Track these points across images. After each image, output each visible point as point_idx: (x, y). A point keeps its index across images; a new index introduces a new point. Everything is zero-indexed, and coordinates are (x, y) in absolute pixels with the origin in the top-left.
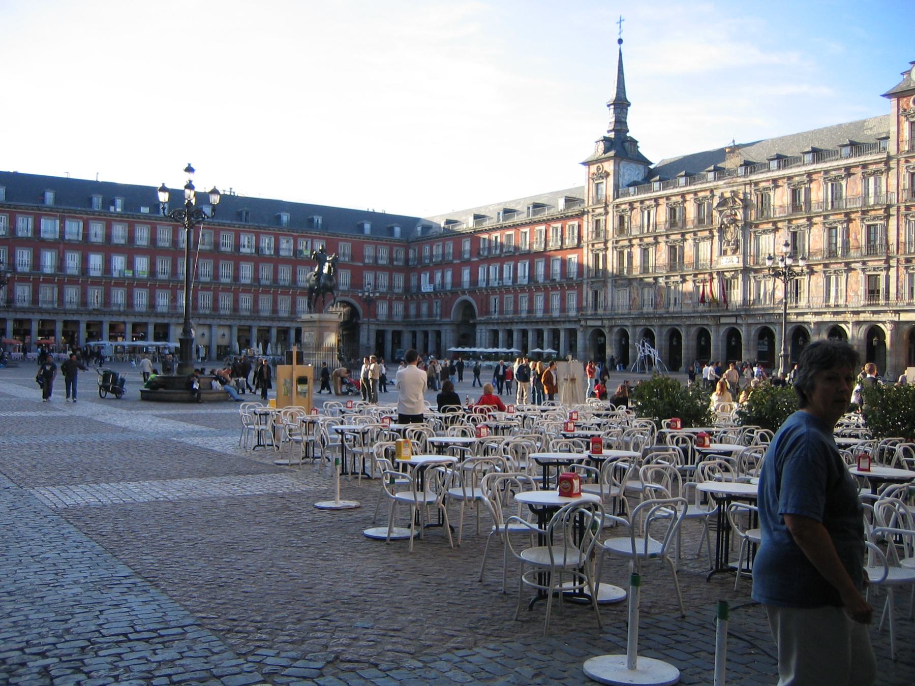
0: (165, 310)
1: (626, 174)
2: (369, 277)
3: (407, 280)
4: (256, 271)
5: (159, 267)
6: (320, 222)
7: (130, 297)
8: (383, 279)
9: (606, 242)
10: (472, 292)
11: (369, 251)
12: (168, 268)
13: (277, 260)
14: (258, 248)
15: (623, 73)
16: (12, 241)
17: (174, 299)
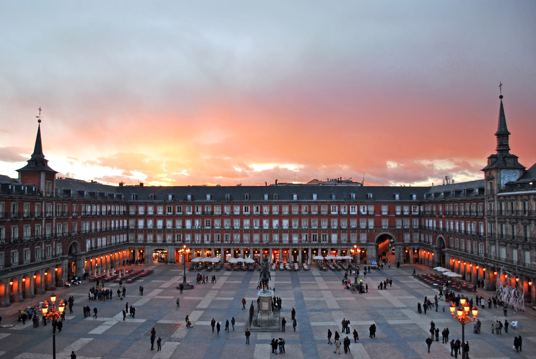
0: (297, 242)
1: (506, 177)
2: (398, 223)
3: (420, 222)
4: (339, 222)
5: (293, 223)
6: (371, 196)
7: (281, 237)
8: (407, 223)
9: (494, 218)
10: (443, 234)
11: (398, 209)
12: (297, 224)
13: (349, 217)
14: (339, 211)
15: (504, 116)
17: (300, 237)
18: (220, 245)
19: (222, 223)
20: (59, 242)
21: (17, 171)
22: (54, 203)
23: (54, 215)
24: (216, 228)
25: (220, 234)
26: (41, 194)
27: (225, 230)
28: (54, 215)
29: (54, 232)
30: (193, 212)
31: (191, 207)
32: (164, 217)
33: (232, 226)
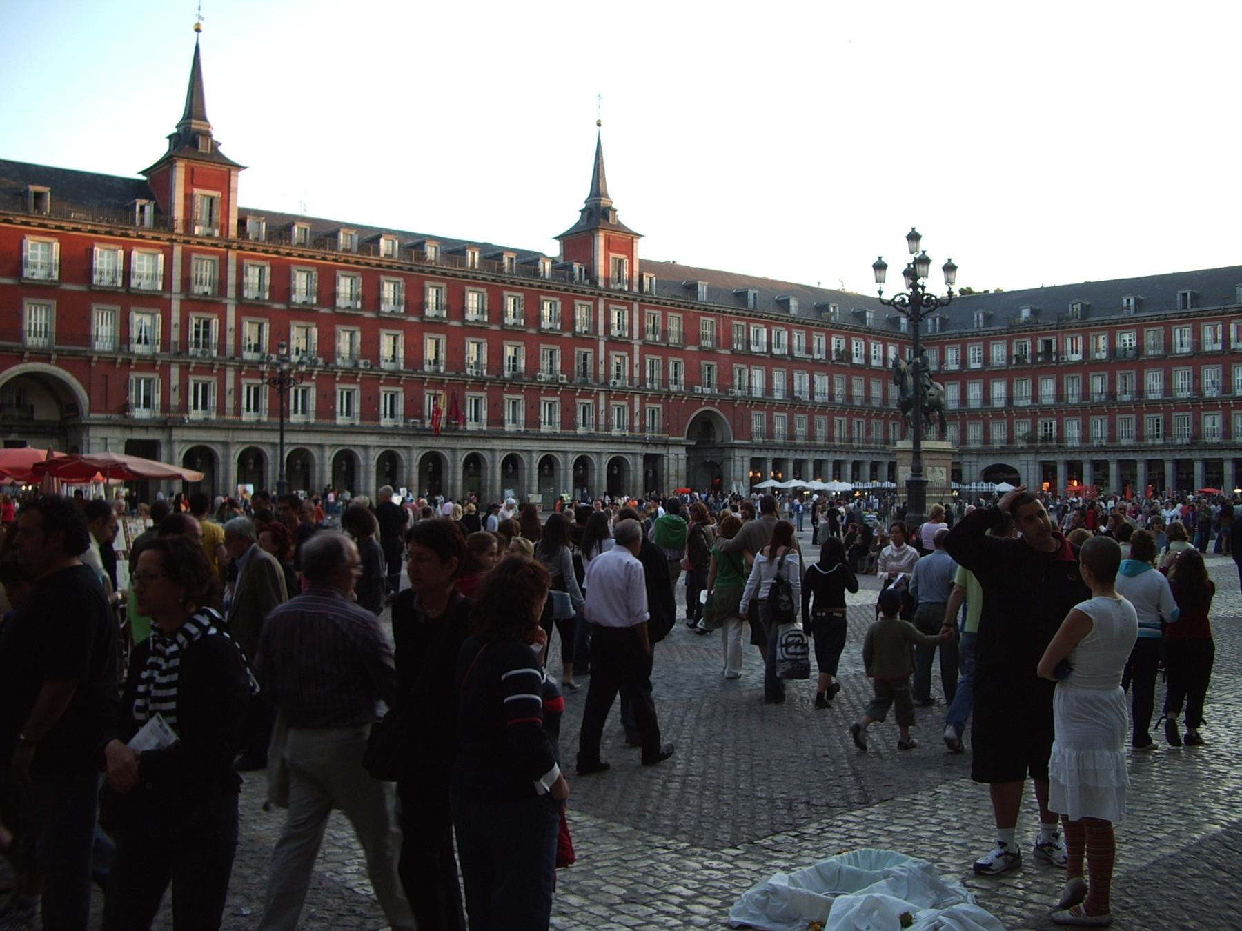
16: (1228, 358)
18: (1162, 449)
19: (1168, 380)
20: (653, 400)
21: (556, 238)
22: (636, 306)
23: (636, 335)
24: (1151, 397)
25: (1161, 416)
26: (594, 282)
27: (1175, 401)
28: (636, 335)
29: (636, 373)
30: (1086, 352)
31: (1080, 338)
32: (1008, 374)
33: (1197, 389)
